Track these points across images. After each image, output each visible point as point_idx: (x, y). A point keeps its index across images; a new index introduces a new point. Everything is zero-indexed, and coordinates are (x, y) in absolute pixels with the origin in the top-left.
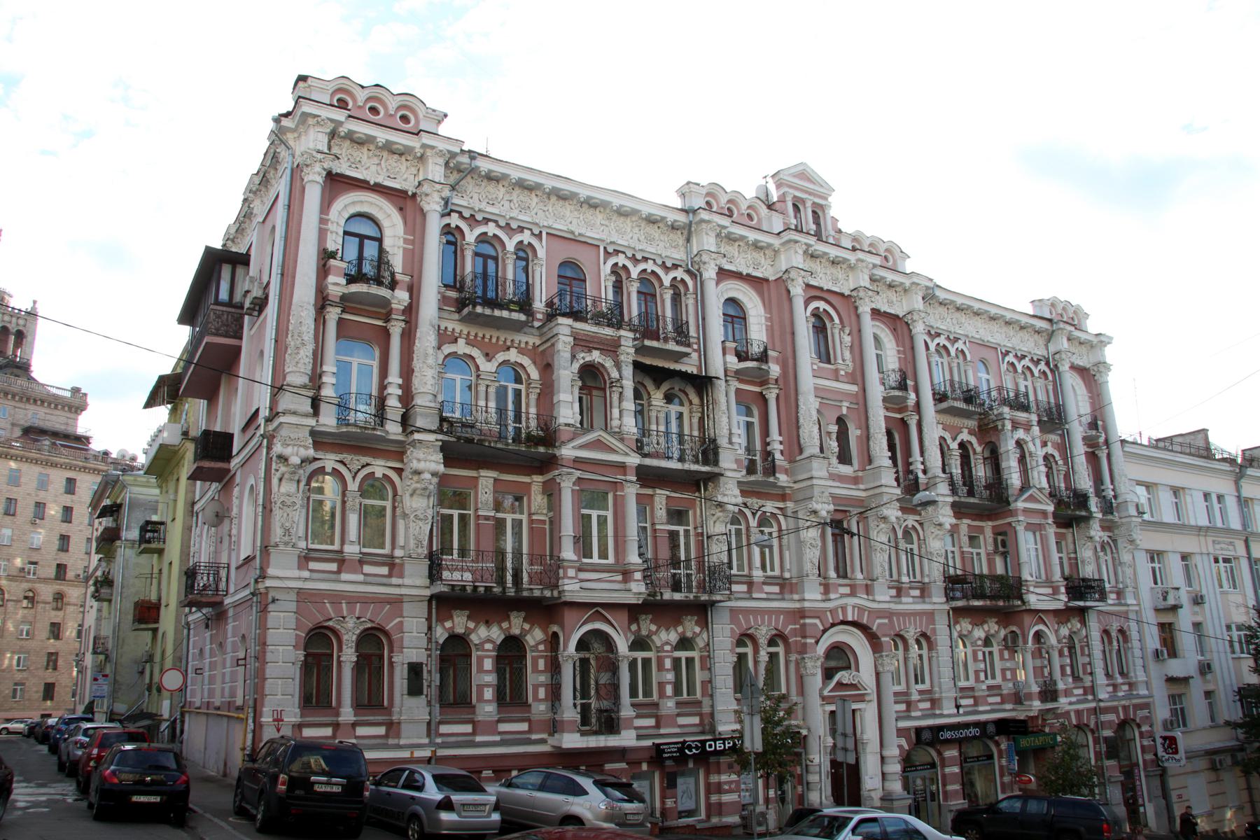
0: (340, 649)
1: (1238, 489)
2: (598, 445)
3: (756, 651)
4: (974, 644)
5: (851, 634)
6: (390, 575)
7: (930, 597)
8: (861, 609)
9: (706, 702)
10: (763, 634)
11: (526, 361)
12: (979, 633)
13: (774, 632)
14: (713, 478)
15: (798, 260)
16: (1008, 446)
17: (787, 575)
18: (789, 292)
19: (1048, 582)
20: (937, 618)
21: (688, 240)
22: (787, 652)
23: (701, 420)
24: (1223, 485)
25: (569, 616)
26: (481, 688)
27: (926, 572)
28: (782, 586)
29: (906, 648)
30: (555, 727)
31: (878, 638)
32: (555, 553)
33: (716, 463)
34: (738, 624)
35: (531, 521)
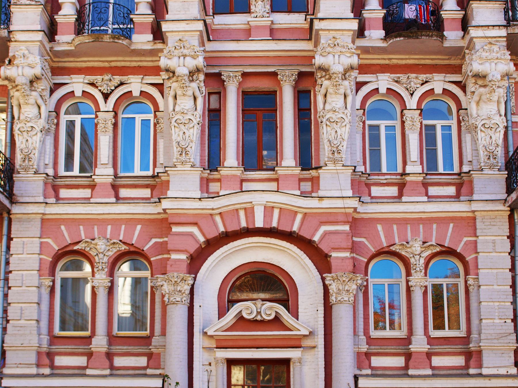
5: (282, 250)
7: (471, 193)
8: (288, 213)
10: (103, 249)
13: (124, 247)
17: (157, 170)
20: (479, 225)
27: (468, 155)
28: (152, 188)
29: (408, 274)
31: (327, 256)
34: (58, 237)
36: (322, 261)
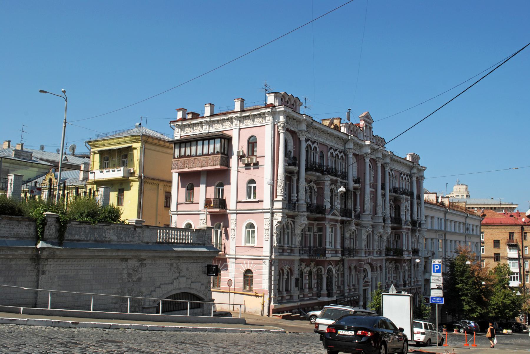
0: (283, 275)
1: (445, 217)
2: (334, 214)
3: (350, 272)
4: (389, 269)
6: (291, 253)
9: (342, 287)
11: (315, 186)
12: (391, 266)
14: (349, 222)
15: (369, 151)
16: (403, 208)
18: (365, 160)
19: (408, 250)
21: (345, 144)
22: (356, 272)
23: (345, 202)
24: (441, 215)
25: (326, 264)
26: (305, 285)
30: (319, 295)
32: (323, 245)
33: (351, 217)
35: (314, 235)
36: (372, 270)
